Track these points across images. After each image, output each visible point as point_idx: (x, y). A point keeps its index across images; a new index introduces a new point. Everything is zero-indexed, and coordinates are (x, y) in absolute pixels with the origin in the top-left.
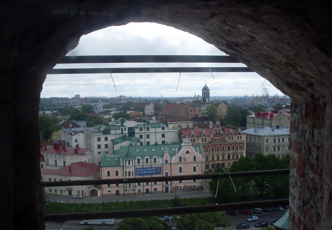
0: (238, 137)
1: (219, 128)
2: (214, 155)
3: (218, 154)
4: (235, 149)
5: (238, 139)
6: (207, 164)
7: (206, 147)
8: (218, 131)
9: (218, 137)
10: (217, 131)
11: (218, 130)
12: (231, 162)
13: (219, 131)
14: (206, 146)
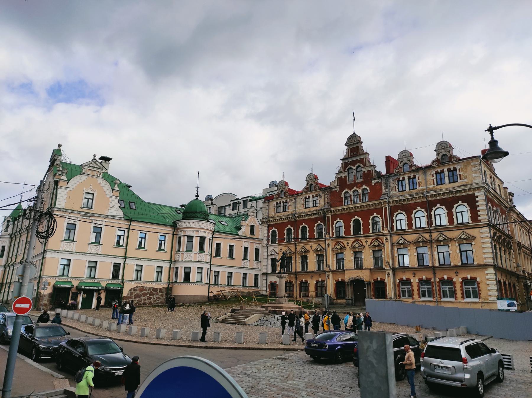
0: (437, 173)
1: (356, 158)
2: (341, 248)
3: (357, 246)
5: (441, 182)
6: (320, 280)
7: (316, 224)
8: (354, 168)
9: (355, 188)
10: (351, 167)
11: (354, 163)
12: (415, 281)
13: (357, 165)
14: (316, 220)
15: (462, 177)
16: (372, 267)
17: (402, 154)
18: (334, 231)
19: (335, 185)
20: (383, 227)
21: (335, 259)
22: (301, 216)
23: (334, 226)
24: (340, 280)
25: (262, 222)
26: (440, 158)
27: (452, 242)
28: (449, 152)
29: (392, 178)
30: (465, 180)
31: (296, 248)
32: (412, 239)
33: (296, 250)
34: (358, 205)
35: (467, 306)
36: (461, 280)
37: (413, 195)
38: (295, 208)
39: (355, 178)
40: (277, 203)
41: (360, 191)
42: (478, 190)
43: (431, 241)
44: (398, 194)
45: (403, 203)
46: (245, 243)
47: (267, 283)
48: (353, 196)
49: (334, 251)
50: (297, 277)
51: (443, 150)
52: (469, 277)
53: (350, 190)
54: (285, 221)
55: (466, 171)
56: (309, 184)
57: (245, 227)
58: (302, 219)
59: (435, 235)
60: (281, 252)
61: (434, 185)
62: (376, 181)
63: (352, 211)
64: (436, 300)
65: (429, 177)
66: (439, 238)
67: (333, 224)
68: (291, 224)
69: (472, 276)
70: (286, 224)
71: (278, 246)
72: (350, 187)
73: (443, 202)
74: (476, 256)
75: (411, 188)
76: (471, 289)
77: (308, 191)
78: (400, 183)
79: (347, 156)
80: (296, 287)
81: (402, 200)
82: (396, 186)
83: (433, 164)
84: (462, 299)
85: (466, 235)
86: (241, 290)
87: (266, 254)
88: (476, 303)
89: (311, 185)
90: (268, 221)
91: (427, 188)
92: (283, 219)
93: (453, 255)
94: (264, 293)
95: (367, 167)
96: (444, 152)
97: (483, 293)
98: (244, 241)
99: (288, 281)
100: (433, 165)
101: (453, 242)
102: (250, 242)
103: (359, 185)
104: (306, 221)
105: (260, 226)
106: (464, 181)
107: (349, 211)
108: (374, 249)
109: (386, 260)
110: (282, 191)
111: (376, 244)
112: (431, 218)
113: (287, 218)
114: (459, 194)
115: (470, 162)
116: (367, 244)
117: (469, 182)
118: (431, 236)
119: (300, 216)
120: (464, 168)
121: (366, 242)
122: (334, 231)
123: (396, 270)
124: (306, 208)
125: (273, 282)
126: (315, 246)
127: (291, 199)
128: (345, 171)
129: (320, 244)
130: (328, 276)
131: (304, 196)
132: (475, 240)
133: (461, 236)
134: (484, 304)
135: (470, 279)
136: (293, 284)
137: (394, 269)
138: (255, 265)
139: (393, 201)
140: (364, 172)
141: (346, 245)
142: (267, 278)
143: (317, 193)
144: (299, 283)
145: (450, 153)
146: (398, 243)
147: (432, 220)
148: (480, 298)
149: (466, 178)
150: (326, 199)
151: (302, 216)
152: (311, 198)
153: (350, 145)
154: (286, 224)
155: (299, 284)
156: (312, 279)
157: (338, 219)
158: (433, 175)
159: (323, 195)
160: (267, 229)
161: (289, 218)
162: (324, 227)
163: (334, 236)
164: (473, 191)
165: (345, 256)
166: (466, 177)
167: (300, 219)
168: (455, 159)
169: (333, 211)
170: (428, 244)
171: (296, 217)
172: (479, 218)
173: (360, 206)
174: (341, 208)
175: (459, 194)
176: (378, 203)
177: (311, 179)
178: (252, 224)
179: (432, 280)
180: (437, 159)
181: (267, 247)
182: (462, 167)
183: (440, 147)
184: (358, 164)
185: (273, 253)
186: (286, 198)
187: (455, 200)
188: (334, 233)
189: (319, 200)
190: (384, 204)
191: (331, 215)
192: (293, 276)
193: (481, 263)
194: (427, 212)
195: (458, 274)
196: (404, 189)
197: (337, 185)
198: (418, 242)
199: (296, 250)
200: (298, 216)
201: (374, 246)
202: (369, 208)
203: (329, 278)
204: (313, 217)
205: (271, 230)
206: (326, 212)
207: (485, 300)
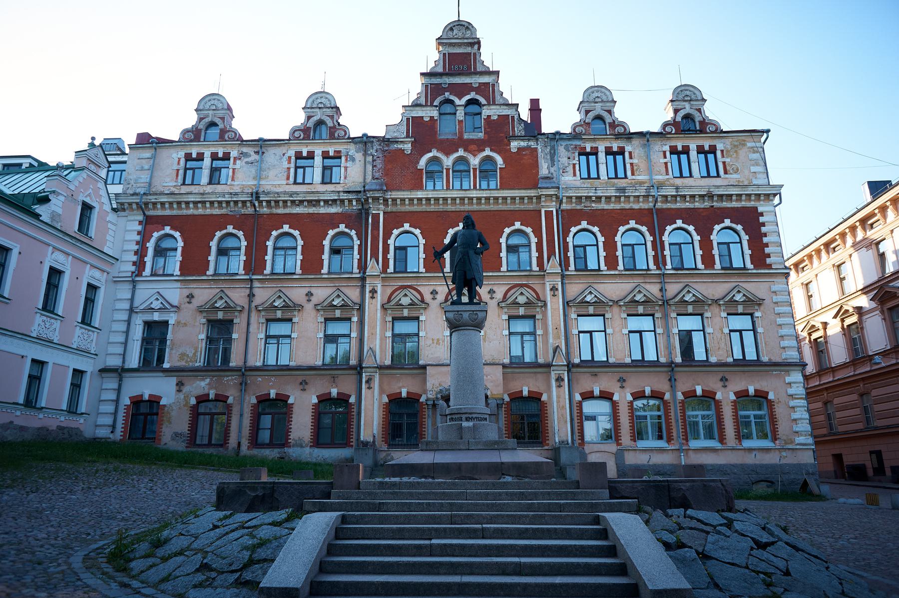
2: (413, 304)
4: (659, 261)
6: (334, 392)
7: (331, 233)
9: (461, 152)
10: (452, 97)
13: (468, 97)
14: (332, 221)
15: (728, 168)
16: (507, 361)
17: (593, 92)
18: (391, 256)
19: (402, 133)
20: (540, 259)
21: (389, 334)
22: (281, 204)
23: (391, 242)
24: (404, 395)
25: (122, 204)
26: (679, 119)
27: (712, 307)
28: (699, 110)
29: (564, 143)
30: (735, 176)
31: (251, 296)
32: (618, 293)
33: (250, 302)
34: (474, 194)
35: (750, 459)
36: (733, 397)
37: (623, 190)
38: (259, 177)
39: (461, 128)
40: (188, 157)
41: (475, 161)
42: (764, 200)
43: (666, 303)
44: (578, 183)
45: (593, 205)
46: (57, 253)
47: (117, 401)
48: (453, 171)
49: (389, 312)
50: (246, 384)
51: (687, 105)
52: (751, 391)
53: (448, 154)
54: (217, 211)
55: (737, 158)
56: (315, 118)
57: (62, 198)
58: (281, 211)
59: (672, 289)
60: (189, 303)
61: (667, 177)
62: (523, 144)
63: (450, 208)
64: (680, 443)
65: (655, 156)
66: (684, 296)
67: (387, 235)
68: (240, 222)
69: (759, 388)
70: (220, 222)
71: (178, 285)
72: (448, 147)
73: (689, 216)
74: (766, 344)
75: (612, 175)
76: (752, 418)
77: (307, 137)
78: (583, 158)
79: (440, 69)
80: (241, 415)
81: (594, 198)
82: (574, 165)
83: (664, 129)
84: (737, 440)
85: (744, 295)
86: (19, 422)
87: (127, 306)
88: (767, 450)
89: (320, 123)
90: (146, 204)
91: (651, 179)
92: (212, 203)
93: (715, 338)
94: (103, 433)
95: (498, 107)
96: (687, 109)
97: (783, 428)
98: (54, 248)
99: (212, 396)
100: (664, 132)
101: (715, 309)
102: (74, 257)
103: (475, 146)
104: (295, 220)
105: (112, 217)
106: (733, 177)
107: (441, 208)
108: (513, 312)
109: (551, 341)
110: (213, 124)
111: (522, 300)
112: (663, 249)
113: (228, 202)
114: (726, 204)
115: (744, 141)
116: (492, 298)
117: (743, 181)
118: (661, 290)
119: (277, 202)
120: (733, 150)
121: (491, 292)
122: (391, 256)
123: (574, 370)
124: (295, 183)
125: (146, 397)
126: (321, 293)
127: (245, 150)
128: (432, 105)
129: (342, 289)
130: (367, 382)
131: (292, 148)
132: (762, 308)
133: (734, 295)
134: (784, 454)
135: (755, 396)
136: (229, 407)
137: (570, 366)
138: (78, 336)
139: (571, 197)
140: (489, 116)
141: (428, 297)
142: (120, 386)
143: (338, 148)
144: (254, 401)
145: (701, 113)
146: (584, 303)
147: (665, 253)
148: (776, 439)
149: (736, 171)
150: (369, 167)
151: (285, 202)
152: (318, 159)
153: (451, 45)
154: (220, 222)
155: (254, 406)
156: (304, 390)
157: (407, 226)
158: (665, 153)
159: (359, 156)
160: (140, 228)
161: (236, 202)
162: (357, 242)
163: (391, 269)
164: (754, 201)
165: (422, 325)
166: (738, 169)
167: (275, 211)
168: (713, 129)
169: (394, 200)
170: (657, 308)
171: (261, 202)
172: (768, 261)
173: (479, 199)
174: (420, 194)
175: (724, 203)
176: (530, 198)
177: (320, 106)
178: (88, 200)
179: (667, 396)
180: (674, 120)
181: (133, 281)
182: (729, 147)
183: (681, 97)
184: (472, 95)
185: (156, 305)
186: (224, 146)
187: (717, 215)
188: (391, 262)
189: (346, 168)
190: (545, 201)
191: (384, 213)
192: (231, 380)
193: (778, 360)
194: (652, 233)
195: (727, 384)
196: (594, 174)
197: (408, 136)
198: (634, 302)
199: (250, 302)
200: (268, 202)
201: (515, 304)
202: (501, 207)
203: (369, 388)
204: (323, 210)
205: (156, 235)
206: (370, 201)
207: (786, 443)
